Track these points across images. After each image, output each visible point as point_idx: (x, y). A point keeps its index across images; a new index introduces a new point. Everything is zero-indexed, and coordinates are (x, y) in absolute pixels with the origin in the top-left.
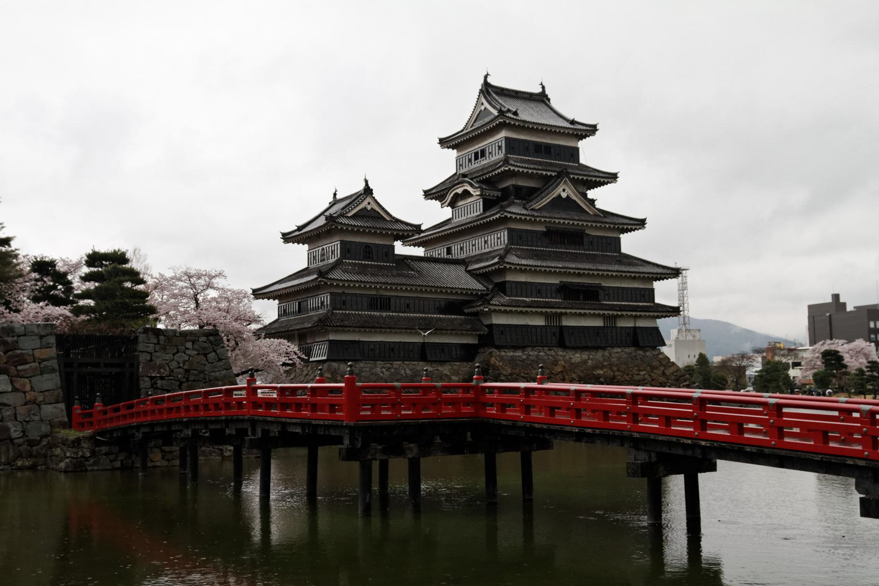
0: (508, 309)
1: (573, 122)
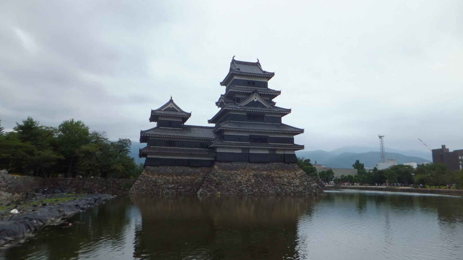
0: (222, 146)
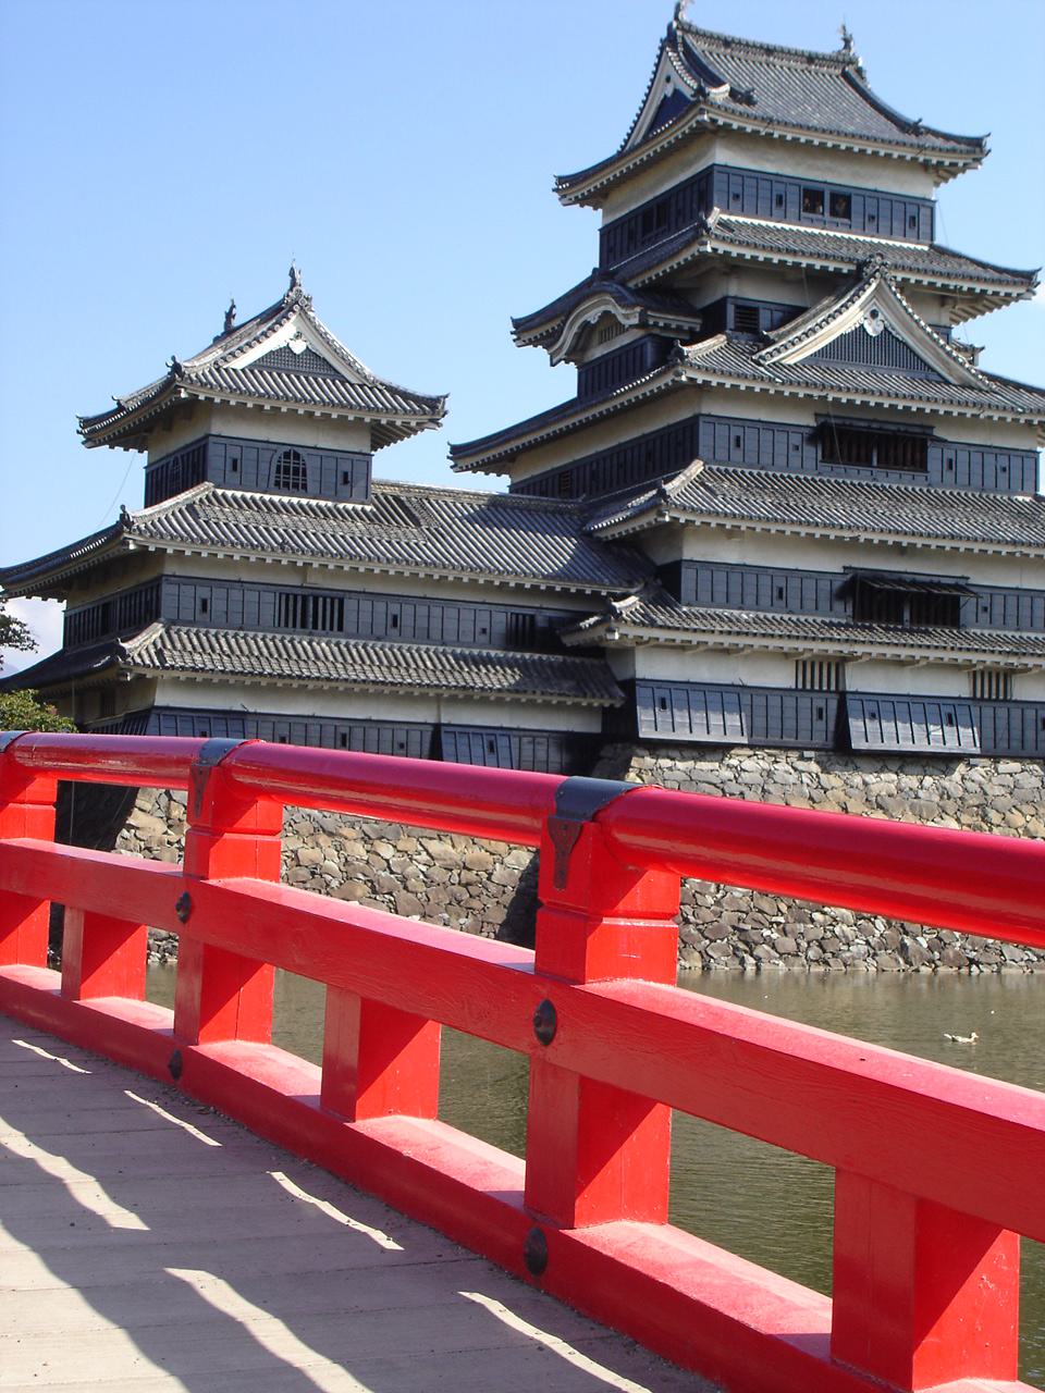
0: (679, 637)
1: (914, 129)
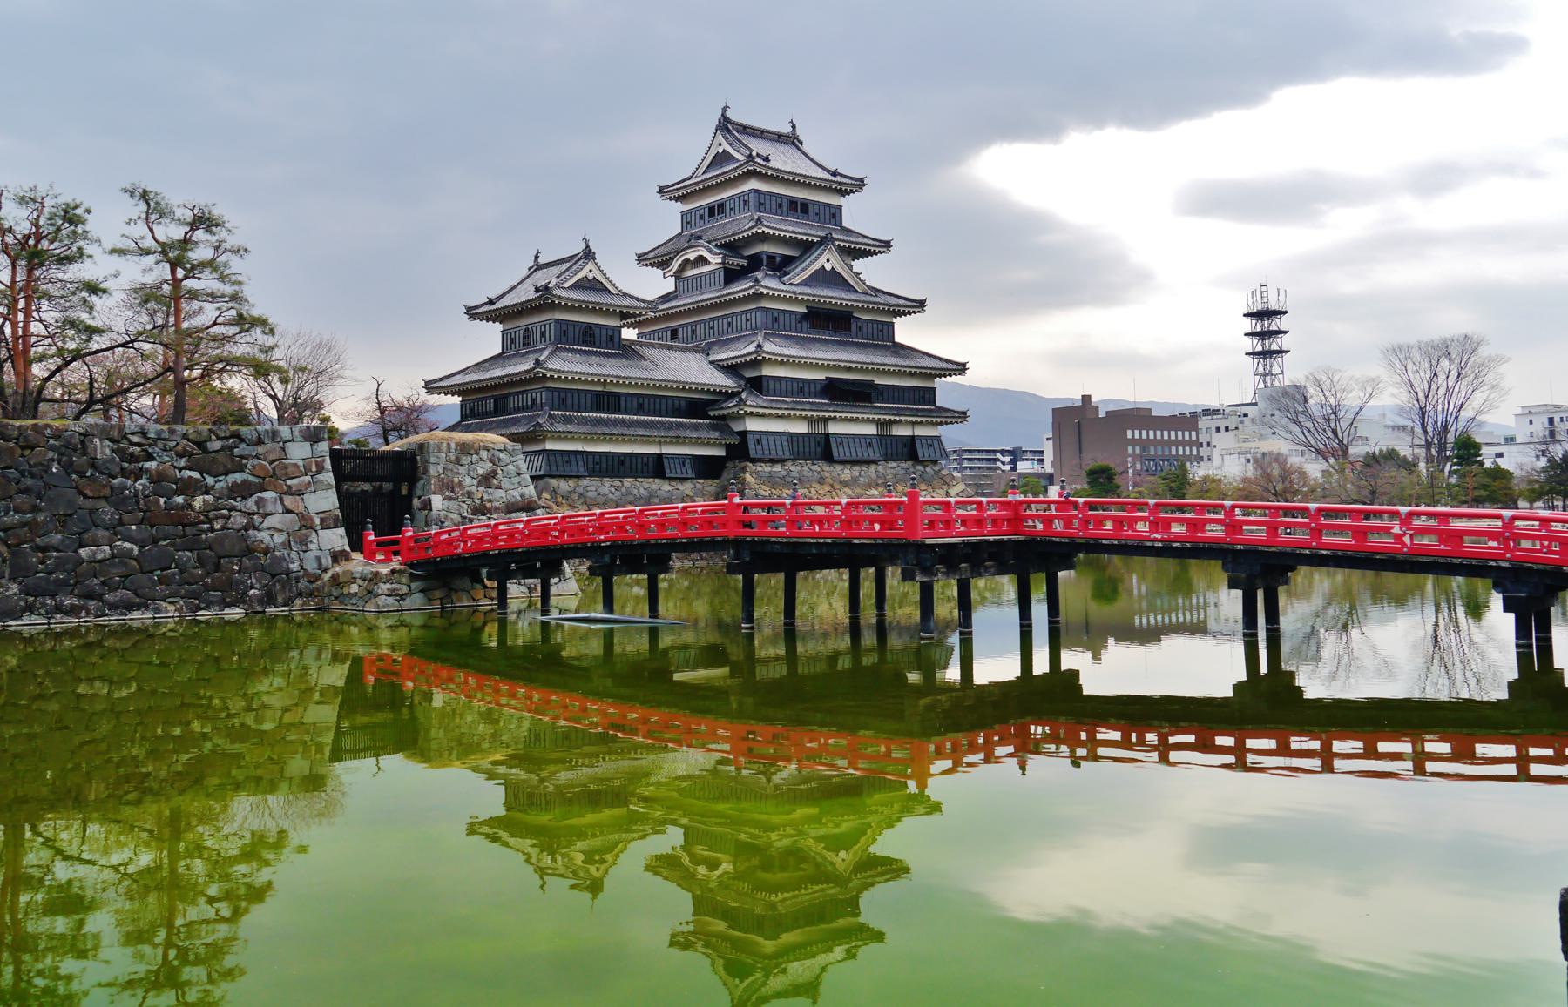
1: (834, 174)
